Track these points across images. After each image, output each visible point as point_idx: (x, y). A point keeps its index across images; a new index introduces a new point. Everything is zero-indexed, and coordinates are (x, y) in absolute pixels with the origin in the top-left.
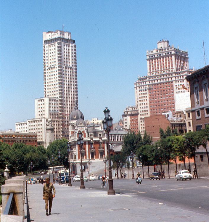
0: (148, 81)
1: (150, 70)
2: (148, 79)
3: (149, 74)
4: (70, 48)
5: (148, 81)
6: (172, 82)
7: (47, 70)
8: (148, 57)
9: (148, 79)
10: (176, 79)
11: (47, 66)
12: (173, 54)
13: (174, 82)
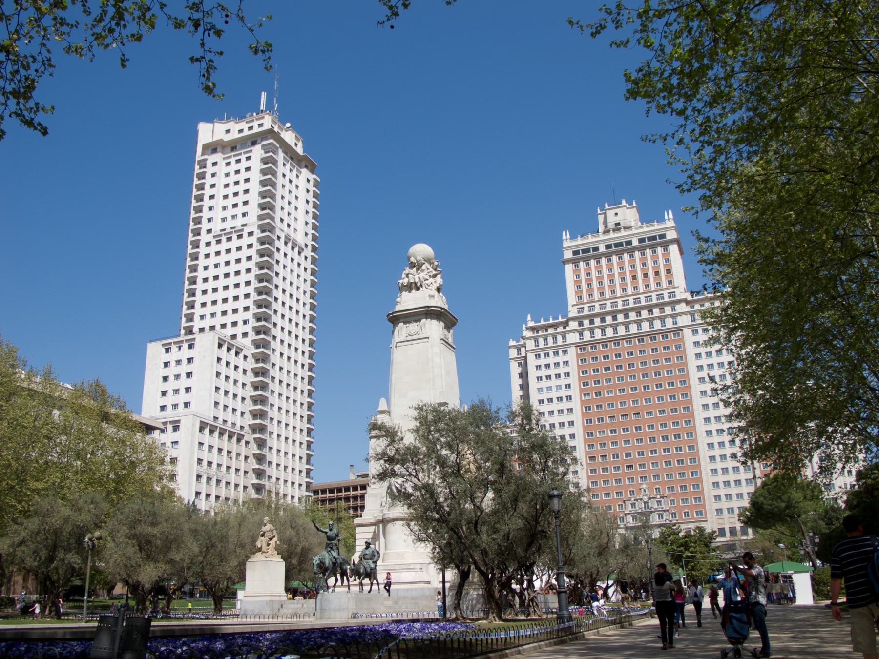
0: (573, 331)
2: (571, 323)
4: (302, 182)
5: (573, 331)
6: (678, 331)
7: (208, 244)
8: (568, 255)
9: (573, 325)
10: (693, 320)
11: (209, 231)
12: (672, 241)
13: (687, 332)
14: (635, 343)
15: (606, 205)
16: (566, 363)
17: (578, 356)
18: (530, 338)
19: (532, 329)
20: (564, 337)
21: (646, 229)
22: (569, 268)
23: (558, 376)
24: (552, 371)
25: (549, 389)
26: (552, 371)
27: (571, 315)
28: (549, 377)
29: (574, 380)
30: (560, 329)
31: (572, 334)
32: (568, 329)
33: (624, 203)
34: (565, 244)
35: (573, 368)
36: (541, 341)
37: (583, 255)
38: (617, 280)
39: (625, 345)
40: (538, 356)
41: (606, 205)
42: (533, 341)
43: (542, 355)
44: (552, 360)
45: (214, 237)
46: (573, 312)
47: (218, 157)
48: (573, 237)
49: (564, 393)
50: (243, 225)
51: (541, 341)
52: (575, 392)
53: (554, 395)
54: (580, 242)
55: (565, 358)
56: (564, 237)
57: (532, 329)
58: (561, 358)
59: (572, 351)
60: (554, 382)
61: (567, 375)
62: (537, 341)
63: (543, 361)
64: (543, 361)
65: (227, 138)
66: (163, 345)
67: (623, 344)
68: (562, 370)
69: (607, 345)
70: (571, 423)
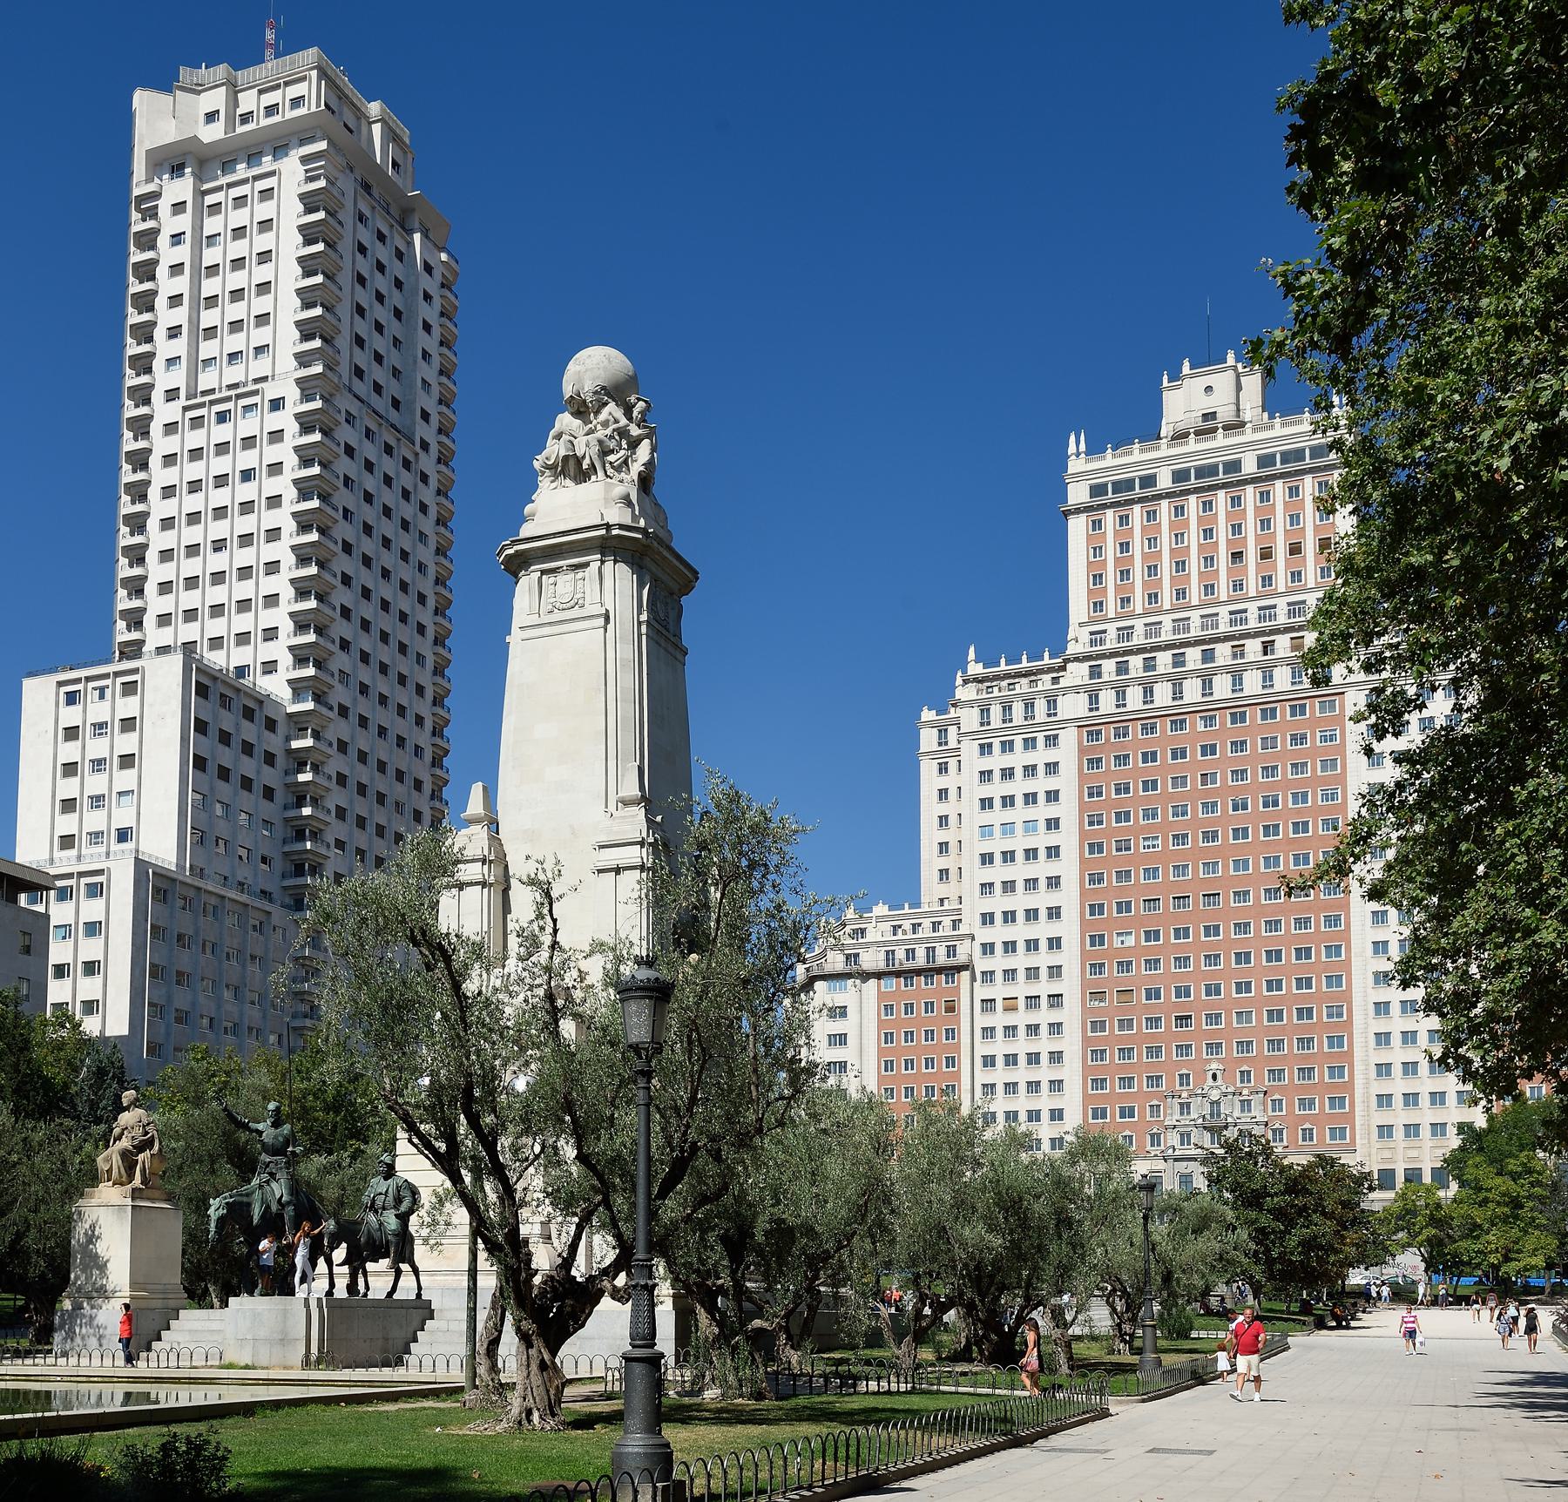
0: (1076, 689)
1: (1098, 606)
3: (1084, 635)
5: (1076, 689)
9: (1077, 673)
14: (1223, 724)
15: (1186, 364)
16: (1052, 768)
17: (1082, 751)
18: (970, 704)
19: (978, 680)
20: (1052, 703)
21: (1279, 429)
22: (1077, 527)
23: (1030, 798)
24: (1018, 787)
25: (1008, 827)
26: (1018, 787)
27: (1072, 649)
28: (1008, 801)
29: (1067, 810)
30: (1045, 681)
31: (1070, 697)
32: (1063, 683)
33: (1231, 358)
34: (1075, 465)
35: (1067, 782)
36: (996, 712)
37: (1117, 495)
38: (1194, 565)
39: (1200, 727)
40: (986, 749)
41: (1186, 369)
42: (976, 711)
43: (997, 747)
44: (1018, 758)
45: (185, 409)
46: (1078, 641)
47: (180, 189)
48: (1094, 450)
49: (1042, 840)
50: (256, 381)
51: (996, 712)
52: (1068, 838)
53: (1019, 844)
54: (1116, 463)
55: (1051, 755)
56: (1072, 449)
57: (978, 680)
58: (1041, 756)
59: (1069, 737)
60: (1019, 813)
61: (1053, 796)
62: (985, 711)
63: (997, 761)
64: (997, 761)
65: (212, 134)
66: (60, 684)
67: (1193, 725)
68: (1041, 784)
69: (1153, 727)
70: (1054, 913)
